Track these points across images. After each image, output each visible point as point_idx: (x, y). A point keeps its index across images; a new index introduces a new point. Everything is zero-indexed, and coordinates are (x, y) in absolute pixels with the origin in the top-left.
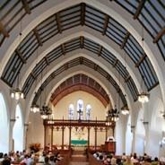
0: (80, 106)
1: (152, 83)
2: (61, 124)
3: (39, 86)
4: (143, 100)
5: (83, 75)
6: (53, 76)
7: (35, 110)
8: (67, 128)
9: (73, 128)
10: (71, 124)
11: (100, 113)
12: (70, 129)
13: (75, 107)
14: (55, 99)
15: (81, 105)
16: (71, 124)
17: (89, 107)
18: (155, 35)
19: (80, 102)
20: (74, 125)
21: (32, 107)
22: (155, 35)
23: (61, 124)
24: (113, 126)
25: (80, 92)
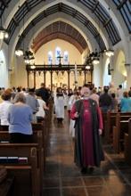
0: (58, 53)
1: (115, 39)
2: (41, 69)
3: (21, 32)
4: (109, 54)
5: (61, 22)
6: (33, 23)
7: (20, 53)
8: (48, 73)
9: (54, 73)
10: (51, 69)
11: (78, 58)
12: (51, 73)
13: (54, 54)
14: (37, 46)
15: (57, 51)
16: (51, 69)
17: (66, 53)
18: (118, 4)
19: (58, 49)
20: (54, 69)
21: (17, 49)
22: (118, 4)
23: (41, 69)
24: (92, 70)
25: (57, 40)
